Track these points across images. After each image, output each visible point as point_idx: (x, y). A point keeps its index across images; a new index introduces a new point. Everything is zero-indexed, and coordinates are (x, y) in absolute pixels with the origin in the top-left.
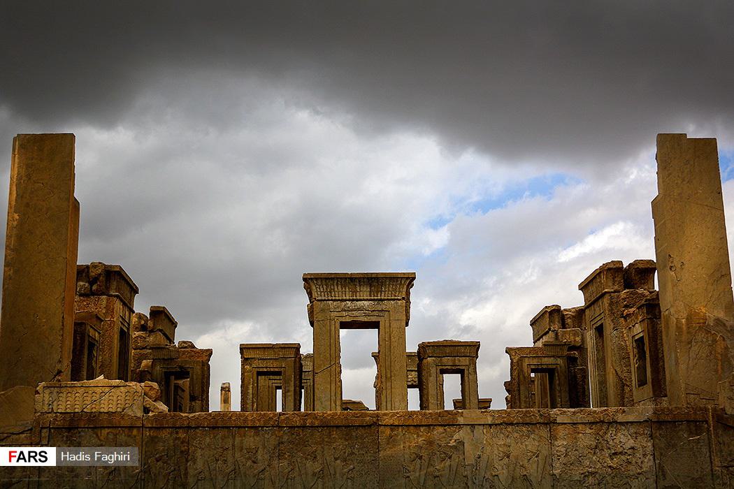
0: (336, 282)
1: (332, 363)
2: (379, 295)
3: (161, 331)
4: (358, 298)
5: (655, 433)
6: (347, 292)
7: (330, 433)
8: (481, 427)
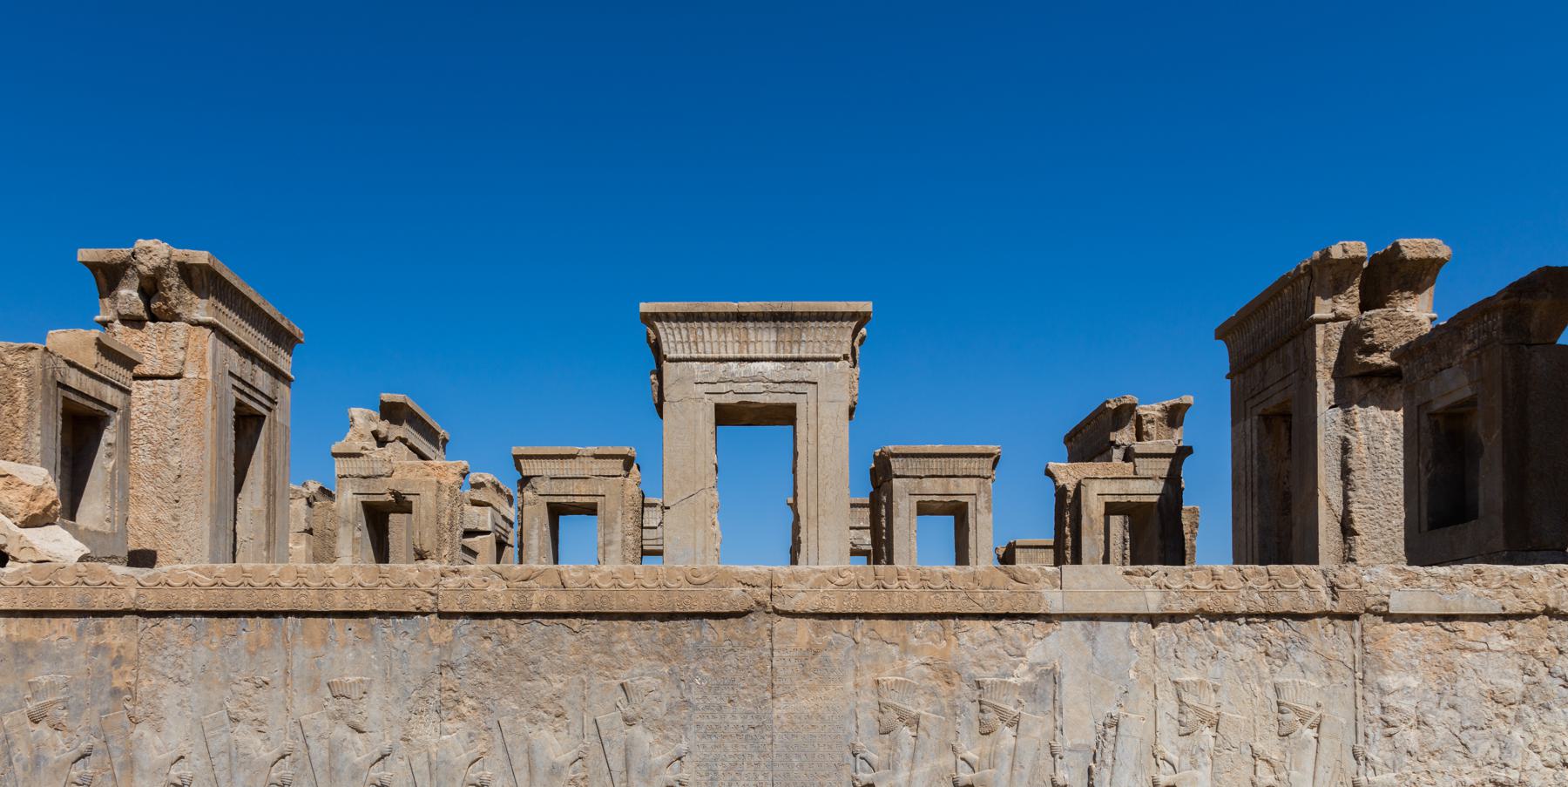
4: (753, 355)
6: (729, 345)
7: (610, 635)
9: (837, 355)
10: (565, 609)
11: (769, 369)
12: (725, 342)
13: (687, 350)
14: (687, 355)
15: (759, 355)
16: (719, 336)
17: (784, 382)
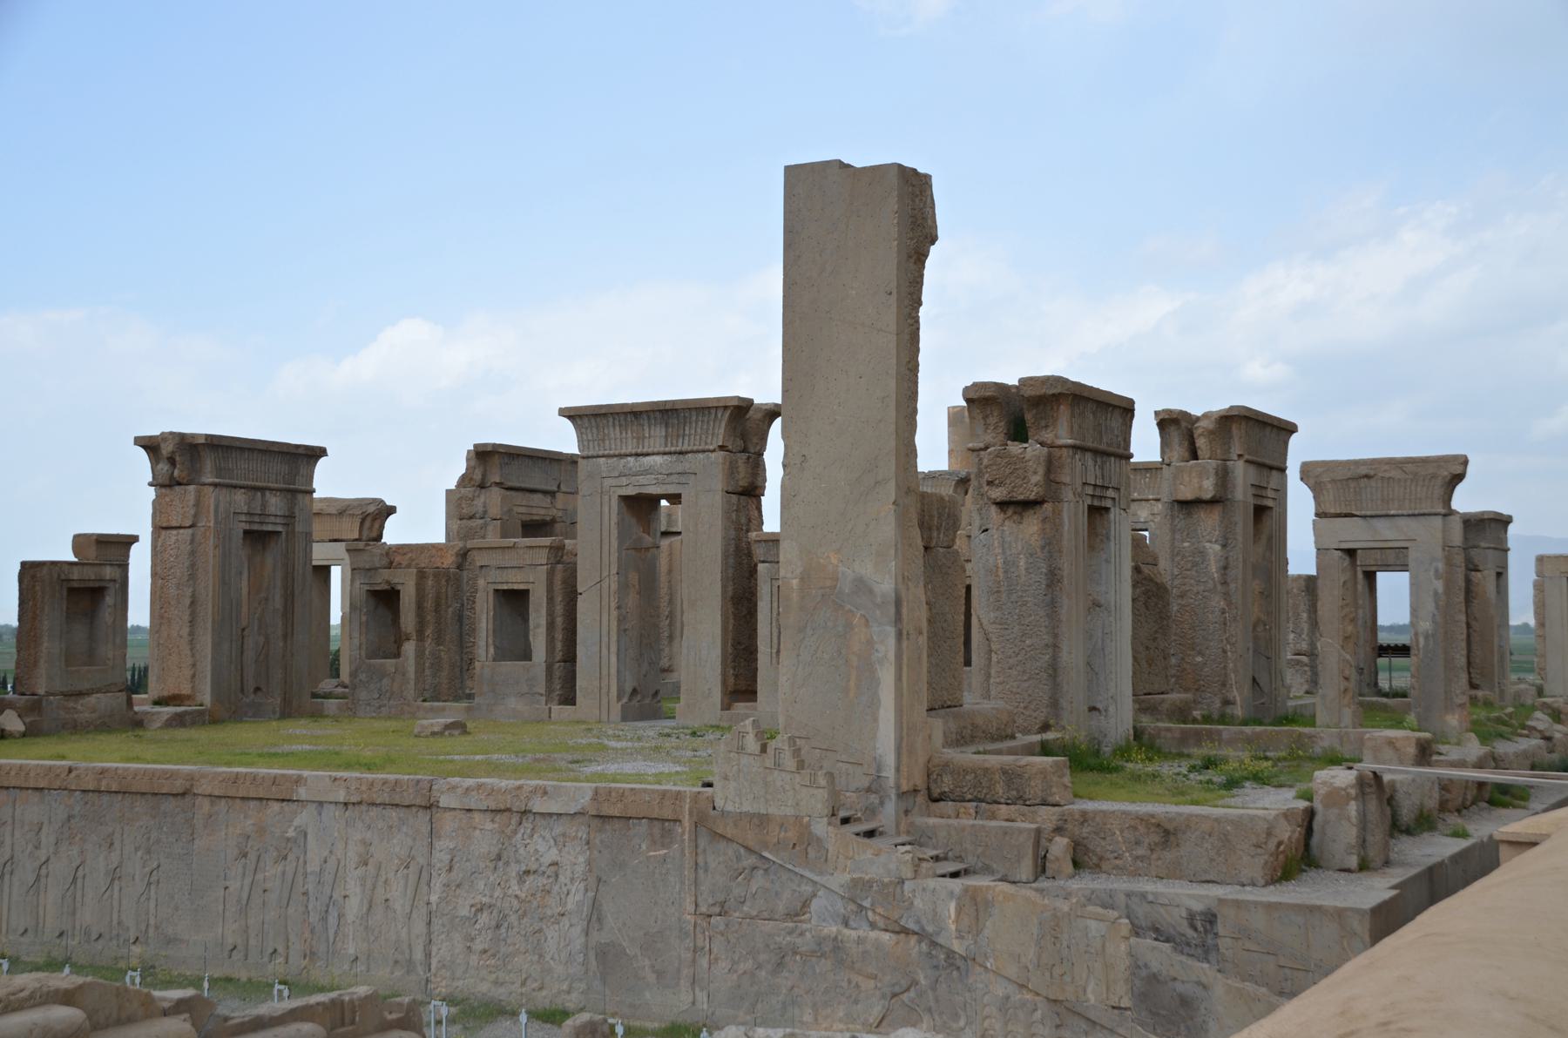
0: (611, 420)
1: (605, 574)
2: (680, 444)
3: (497, 484)
4: (645, 450)
5: (594, 838)
6: (630, 441)
8: (332, 807)
9: (711, 448)
10: (113, 790)
11: (658, 463)
12: (626, 439)
13: (597, 449)
14: (595, 454)
15: (650, 450)
16: (621, 433)
17: (671, 474)
